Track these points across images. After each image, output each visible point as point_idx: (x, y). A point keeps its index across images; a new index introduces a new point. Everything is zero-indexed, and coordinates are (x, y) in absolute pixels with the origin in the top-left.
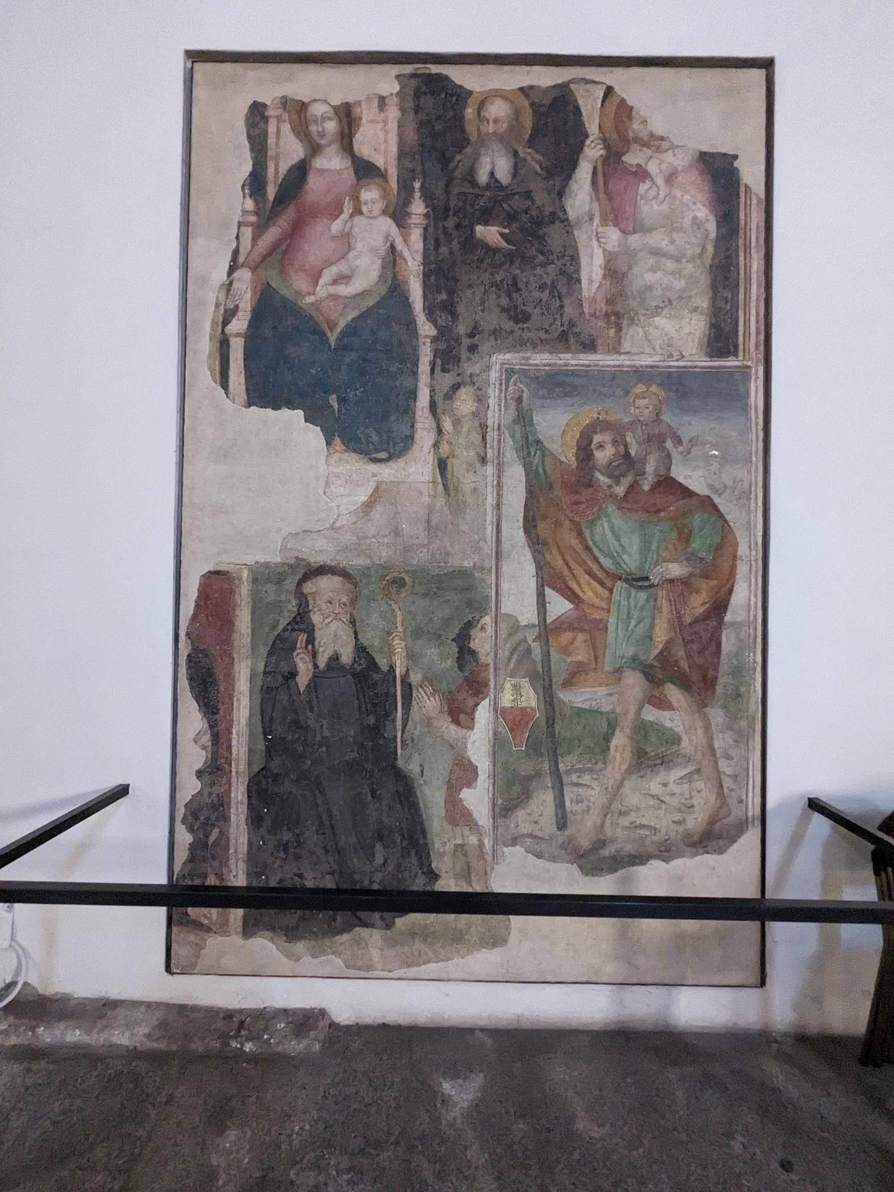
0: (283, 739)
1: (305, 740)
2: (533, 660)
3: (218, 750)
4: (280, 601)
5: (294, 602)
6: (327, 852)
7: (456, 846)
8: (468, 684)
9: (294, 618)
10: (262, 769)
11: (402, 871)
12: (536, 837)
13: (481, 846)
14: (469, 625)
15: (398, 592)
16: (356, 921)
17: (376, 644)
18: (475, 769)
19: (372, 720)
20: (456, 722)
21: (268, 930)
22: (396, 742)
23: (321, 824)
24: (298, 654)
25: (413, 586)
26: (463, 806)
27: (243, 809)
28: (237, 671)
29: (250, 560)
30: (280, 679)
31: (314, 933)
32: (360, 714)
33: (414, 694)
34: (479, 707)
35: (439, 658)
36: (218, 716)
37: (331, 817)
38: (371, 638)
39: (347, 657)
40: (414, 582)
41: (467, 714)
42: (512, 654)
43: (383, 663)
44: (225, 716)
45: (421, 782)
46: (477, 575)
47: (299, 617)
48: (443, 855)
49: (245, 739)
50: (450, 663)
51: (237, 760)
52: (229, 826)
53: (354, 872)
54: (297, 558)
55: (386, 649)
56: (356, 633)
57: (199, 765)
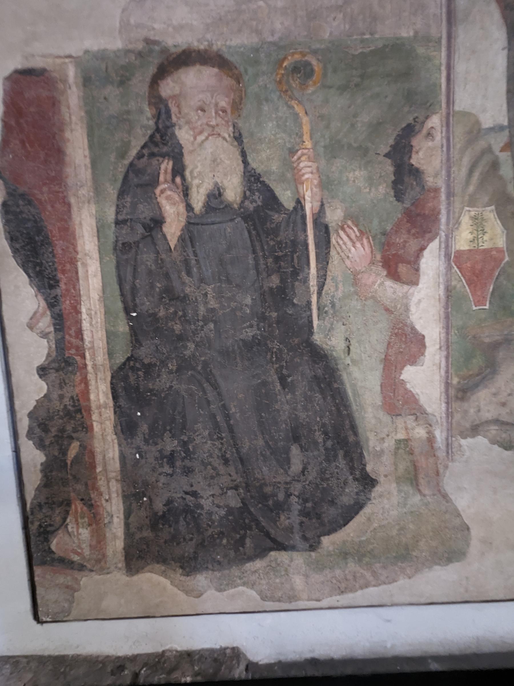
0: (154, 315)
1: (185, 315)
2: (501, 178)
3: (63, 338)
4: (128, 112)
5: (148, 112)
6: (226, 461)
7: (398, 442)
8: (410, 218)
9: (152, 137)
10: (129, 359)
11: (328, 479)
12: (504, 423)
13: (431, 440)
14: (409, 131)
15: (303, 86)
16: (269, 543)
17: (274, 168)
18: (420, 341)
19: (275, 281)
20: (394, 275)
21: (158, 563)
22: (310, 310)
23: (217, 426)
24: (162, 192)
25: (325, 75)
26: (406, 389)
27: (109, 413)
28: (77, 222)
29: (75, 48)
30: (140, 230)
31: (219, 563)
32: (258, 273)
33: (333, 241)
34: (426, 253)
35: (367, 185)
36: (58, 291)
37: (227, 417)
38: (266, 160)
39: (233, 190)
40: (325, 68)
41: (409, 263)
42: (471, 172)
43: (286, 197)
44: (67, 290)
45: (348, 361)
46: (421, 50)
47: (158, 136)
48: (379, 454)
49: (99, 318)
50: (383, 190)
51: (93, 347)
52: (92, 437)
53: (265, 485)
54: (148, 41)
55: (289, 175)
56: (244, 154)
57: (40, 359)
